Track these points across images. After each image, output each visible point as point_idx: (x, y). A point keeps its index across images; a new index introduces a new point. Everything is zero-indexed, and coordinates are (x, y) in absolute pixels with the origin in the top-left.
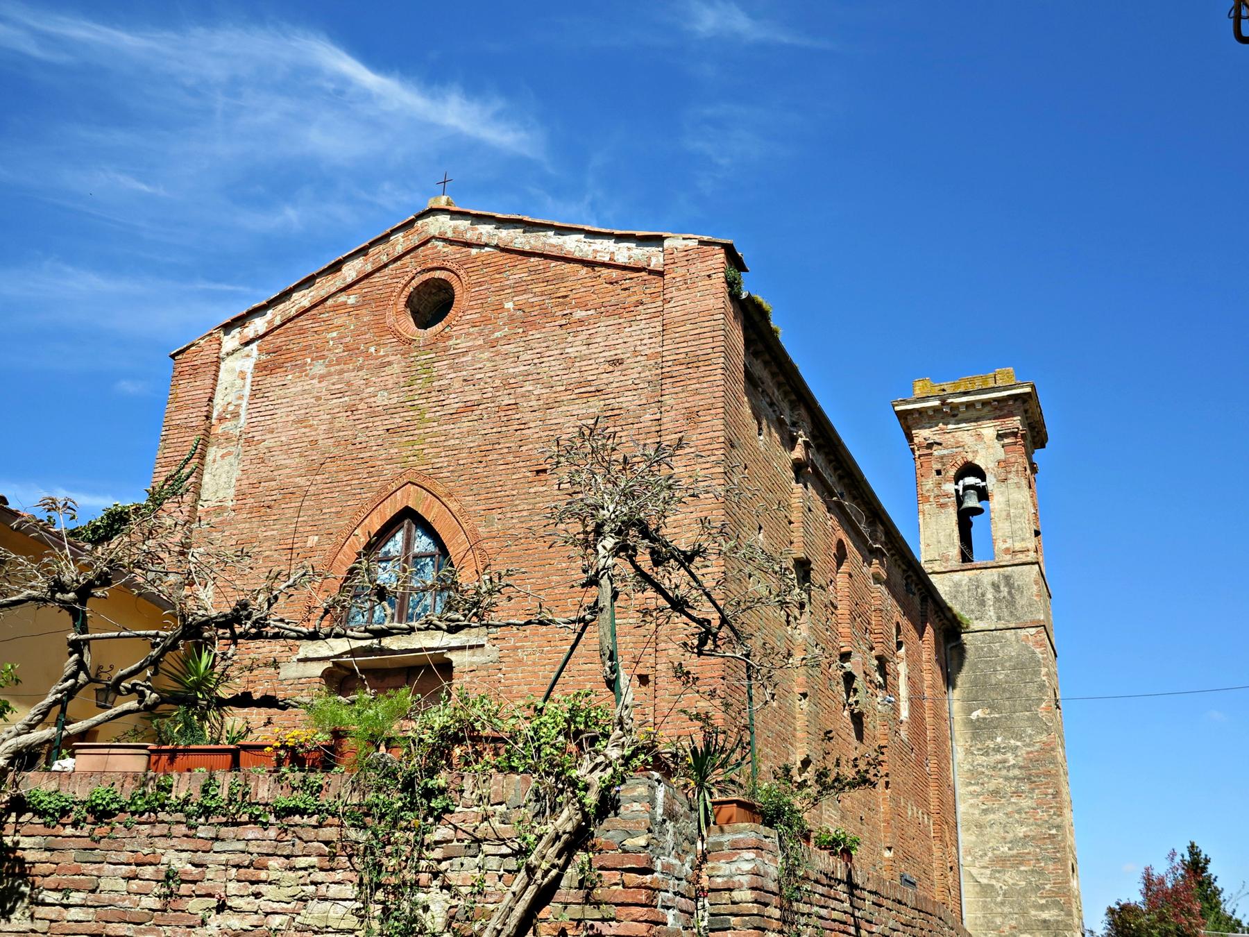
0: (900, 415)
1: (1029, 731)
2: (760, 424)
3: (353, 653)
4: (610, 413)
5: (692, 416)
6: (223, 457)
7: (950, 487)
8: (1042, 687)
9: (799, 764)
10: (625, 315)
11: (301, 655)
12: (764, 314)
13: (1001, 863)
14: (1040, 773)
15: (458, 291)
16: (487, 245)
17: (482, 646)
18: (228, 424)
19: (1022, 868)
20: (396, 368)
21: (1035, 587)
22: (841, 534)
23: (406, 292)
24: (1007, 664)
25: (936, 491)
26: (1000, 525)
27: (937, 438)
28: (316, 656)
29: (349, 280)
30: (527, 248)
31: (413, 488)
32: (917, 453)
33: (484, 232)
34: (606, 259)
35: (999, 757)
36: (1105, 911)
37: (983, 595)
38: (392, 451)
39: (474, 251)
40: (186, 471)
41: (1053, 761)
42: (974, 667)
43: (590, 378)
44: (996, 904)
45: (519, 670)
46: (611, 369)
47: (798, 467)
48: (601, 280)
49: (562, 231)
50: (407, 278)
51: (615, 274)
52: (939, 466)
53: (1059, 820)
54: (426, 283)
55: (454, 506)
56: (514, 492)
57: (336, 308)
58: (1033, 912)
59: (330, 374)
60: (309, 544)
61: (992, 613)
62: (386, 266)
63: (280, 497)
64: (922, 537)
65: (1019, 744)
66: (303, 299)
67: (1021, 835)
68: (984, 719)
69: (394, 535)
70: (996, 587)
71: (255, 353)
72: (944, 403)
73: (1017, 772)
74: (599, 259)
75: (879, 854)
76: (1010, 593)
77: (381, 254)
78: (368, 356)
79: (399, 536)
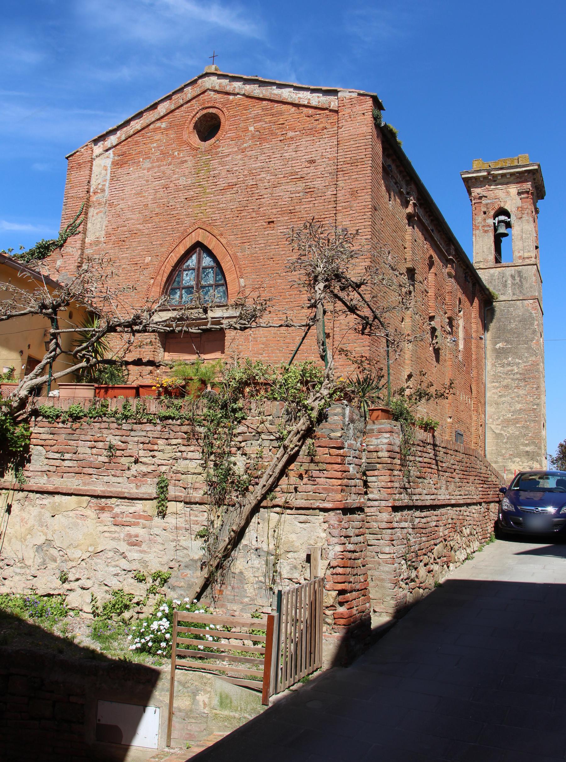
0: (466, 180)
1: (526, 355)
2: (390, 195)
4: (308, 190)
5: (354, 193)
6: (97, 213)
7: (491, 221)
8: (534, 332)
9: (406, 377)
10: (317, 135)
12: (393, 135)
13: (507, 423)
14: (530, 377)
15: (222, 120)
16: (238, 94)
18: (99, 195)
19: (518, 425)
20: (190, 164)
21: (534, 278)
22: (432, 252)
24: (517, 319)
25: (483, 224)
26: (517, 243)
27: (485, 194)
29: (162, 114)
30: (261, 96)
31: (201, 231)
32: (473, 202)
33: (236, 86)
34: (306, 103)
35: (509, 368)
36: (558, 445)
37: (506, 282)
38: (189, 210)
39: (231, 97)
40: (78, 222)
41: (538, 371)
42: (499, 320)
43: (297, 170)
44: (503, 443)
46: (309, 165)
47: (410, 217)
48: (302, 115)
49: (280, 86)
50: (194, 113)
51: (310, 111)
52: (485, 210)
53: (538, 401)
54: (204, 116)
55: (224, 241)
56: (256, 234)
57: (155, 130)
58: (521, 447)
59: (153, 167)
60: (146, 261)
61: (510, 292)
62: (182, 106)
63: (129, 235)
64: (474, 248)
65: (520, 361)
66: (136, 125)
67: (518, 408)
68: (503, 348)
69: (191, 257)
70: (513, 277)
71: (112, 155)
72: (489, 174)
73: (518, 376)
74: (301, 103)
75: (445, 420)
76: (520, 281)
77: (179, 99)
78: (174, 157)
79: (194, 257)
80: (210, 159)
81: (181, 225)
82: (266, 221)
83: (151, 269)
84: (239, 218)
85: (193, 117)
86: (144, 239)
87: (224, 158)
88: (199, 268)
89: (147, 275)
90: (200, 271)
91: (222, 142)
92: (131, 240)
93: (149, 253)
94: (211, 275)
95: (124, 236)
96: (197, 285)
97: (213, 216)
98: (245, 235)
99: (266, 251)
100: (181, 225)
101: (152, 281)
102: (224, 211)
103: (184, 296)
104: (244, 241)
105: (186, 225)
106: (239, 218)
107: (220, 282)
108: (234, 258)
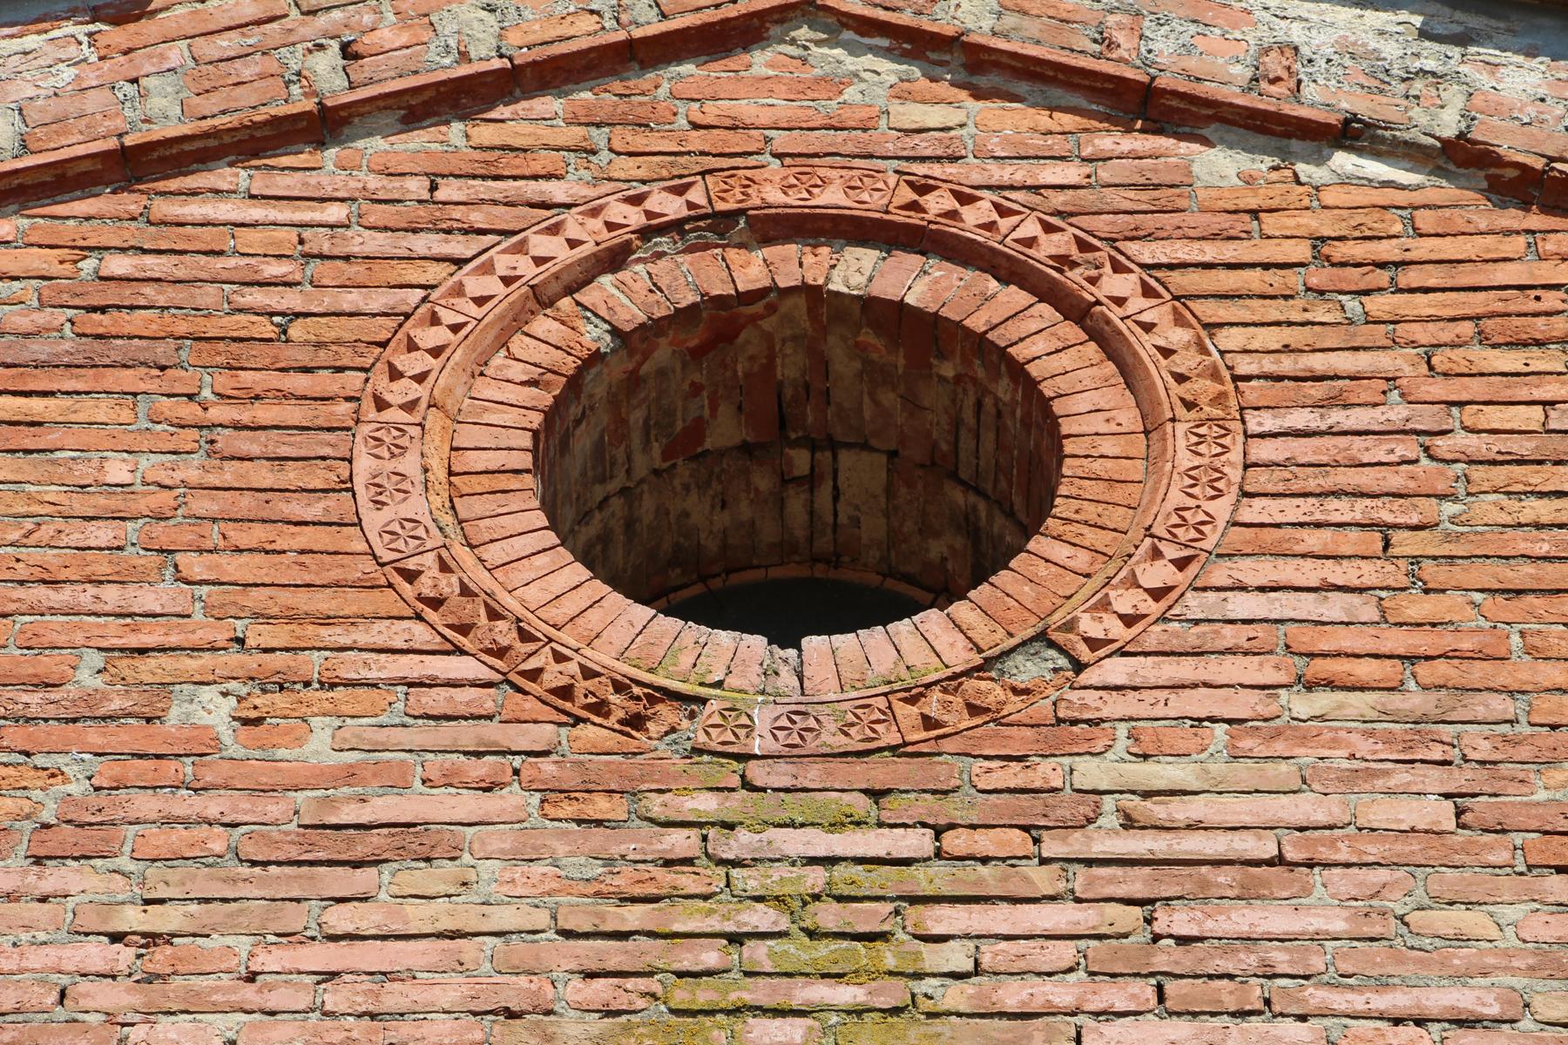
16: (1350, 133)
23: (552, 341)
39: (1220, 167)
54: (718, 322)
62: (325, 125)
80: (924, 879)
85: (541, 298)
87: (1202, 897)
91: (1116, 670)
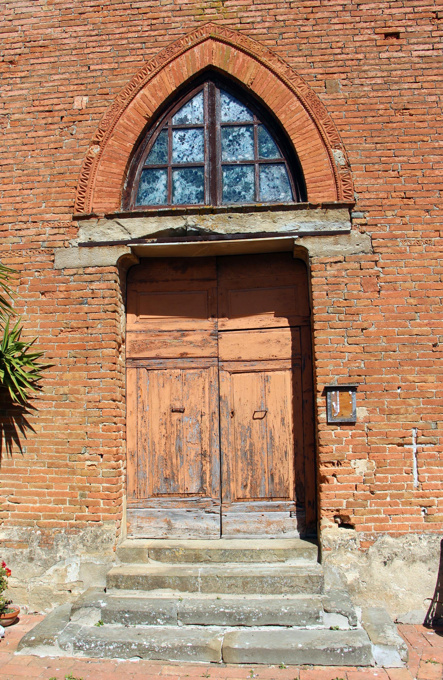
3: (160, 236)
11: (83, 239)
17: (347, 232)
28: (105, 240)
31: (215, 45)
45: (402, 263)
56: (361, 56)
63: (27, 50)
69: (190, 100)
81: (162, 32)
82: (378, 30)
83: (90, 124)
84: (312, 22)
86: (67, 58)
88: (213, 125)
89: (82, 136)
90: (212, 130)
92: (32, 61)
93: (83, 87)
94: (246, 141)
95: (12, 52)
96: (213, 159)
97: (245, 15)
98: (332, 58)
99: (390, 93)
100: (162, 32)
101: (96, 150)
102: (271, 6)
103: (177, 184)
104: (331, 70)
105: (175, 31)
106: (312, 22)
107: (272, 157)
108: (312, 107)
